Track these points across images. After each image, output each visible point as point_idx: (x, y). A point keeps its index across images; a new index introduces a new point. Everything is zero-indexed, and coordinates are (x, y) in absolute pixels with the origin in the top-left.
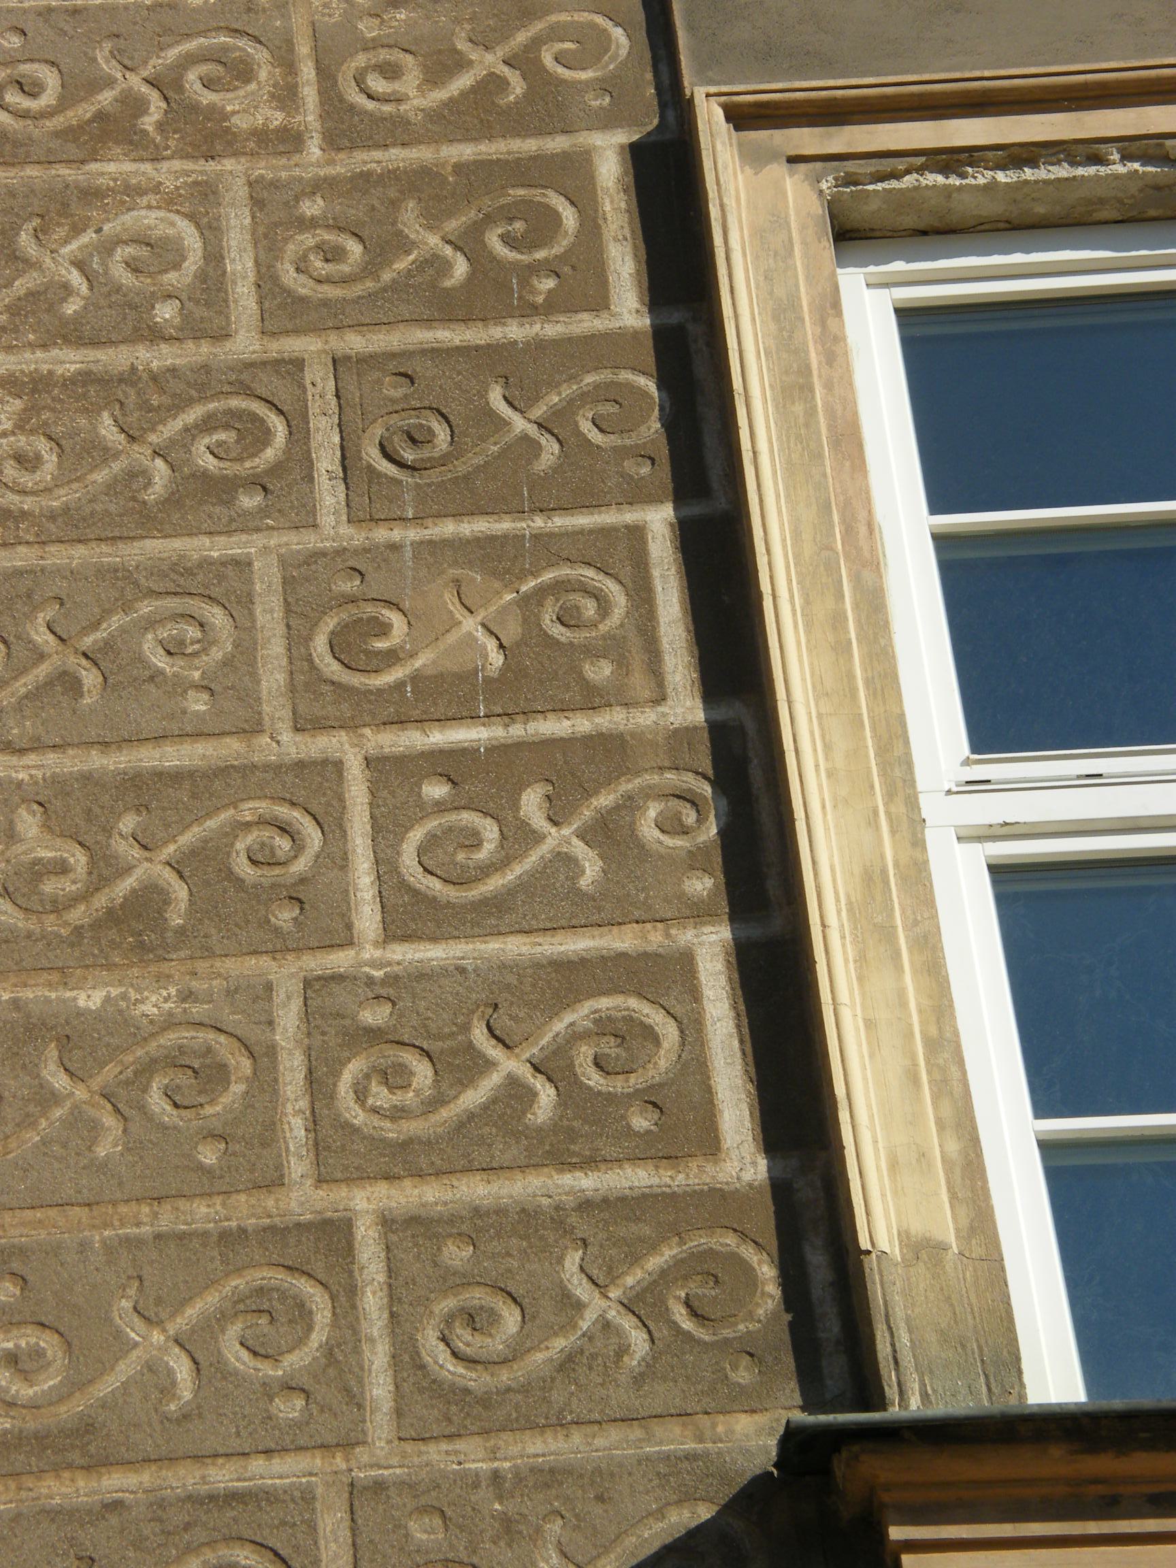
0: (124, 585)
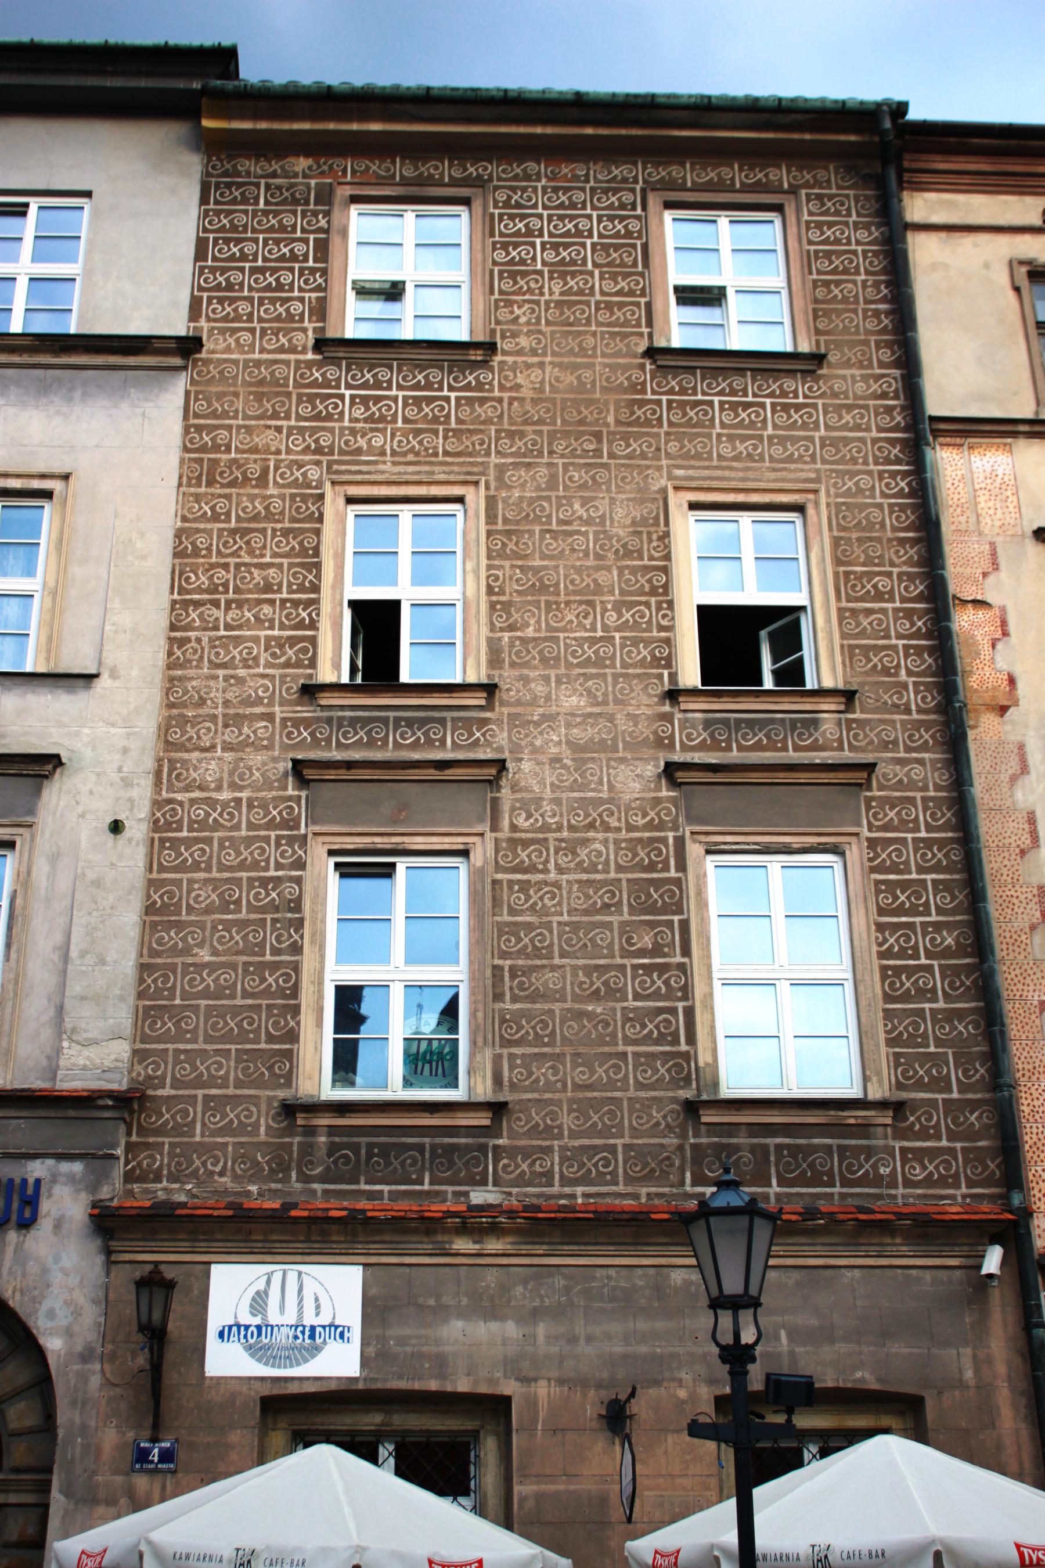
0: (594, 925)
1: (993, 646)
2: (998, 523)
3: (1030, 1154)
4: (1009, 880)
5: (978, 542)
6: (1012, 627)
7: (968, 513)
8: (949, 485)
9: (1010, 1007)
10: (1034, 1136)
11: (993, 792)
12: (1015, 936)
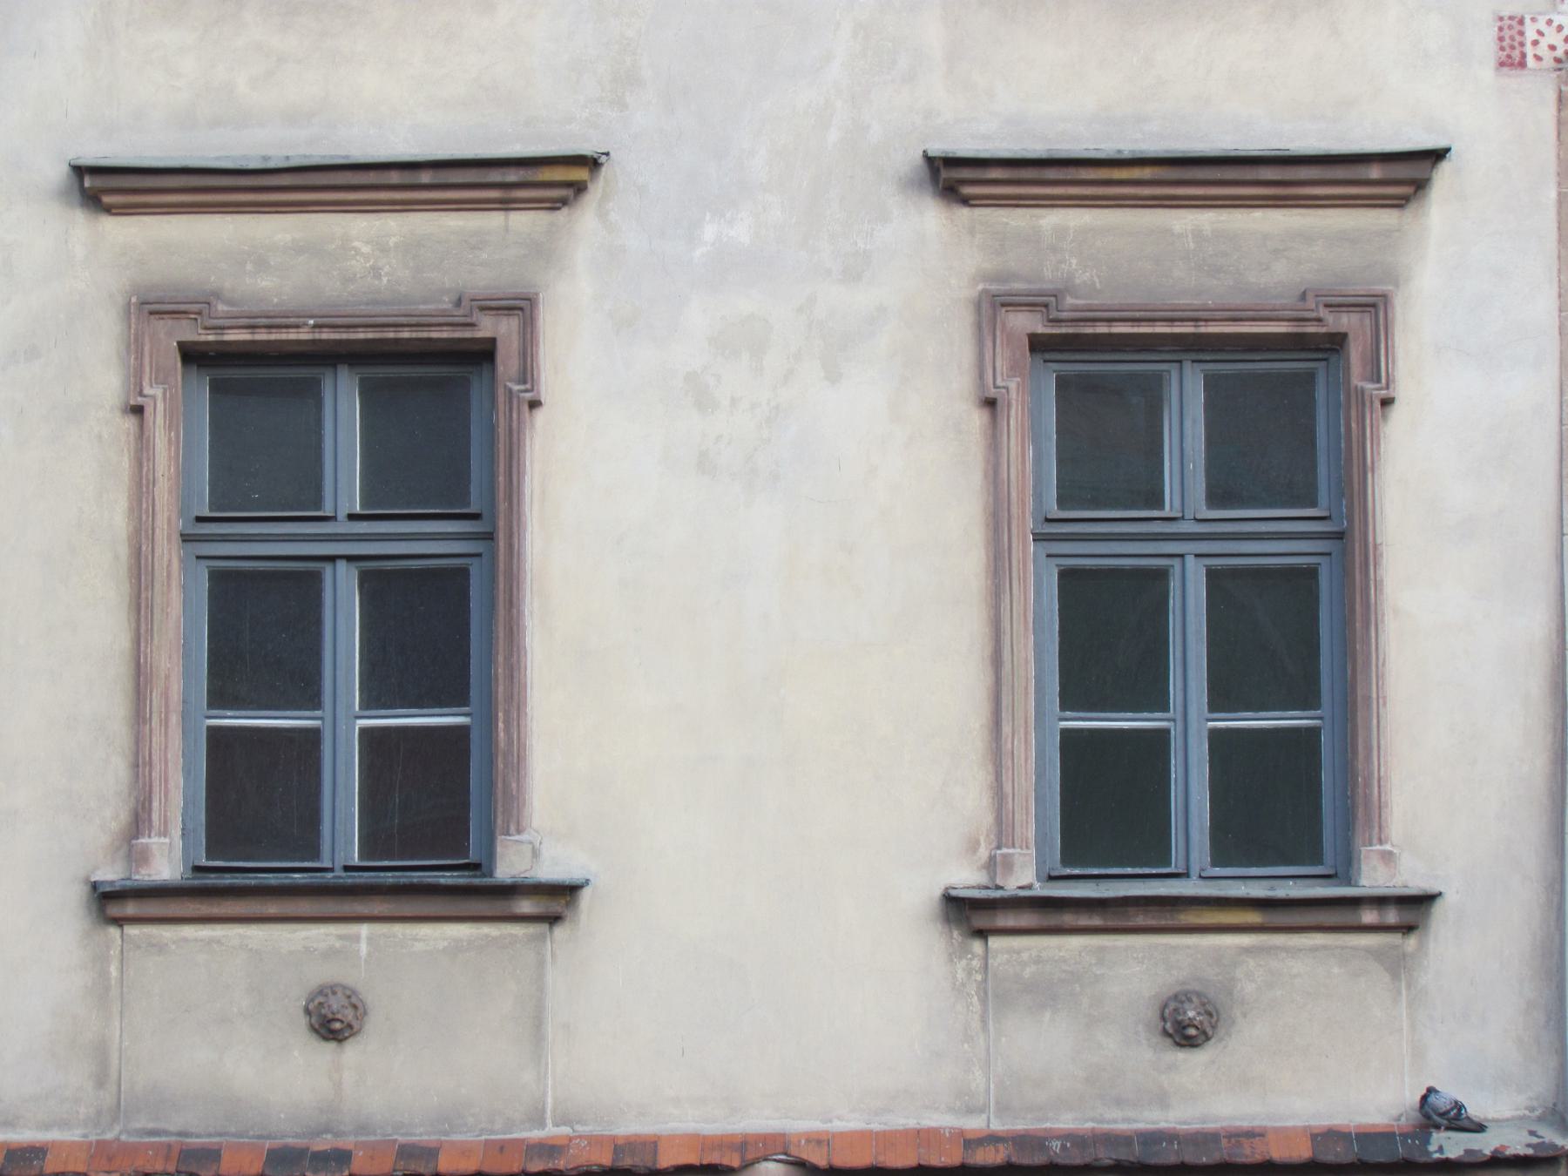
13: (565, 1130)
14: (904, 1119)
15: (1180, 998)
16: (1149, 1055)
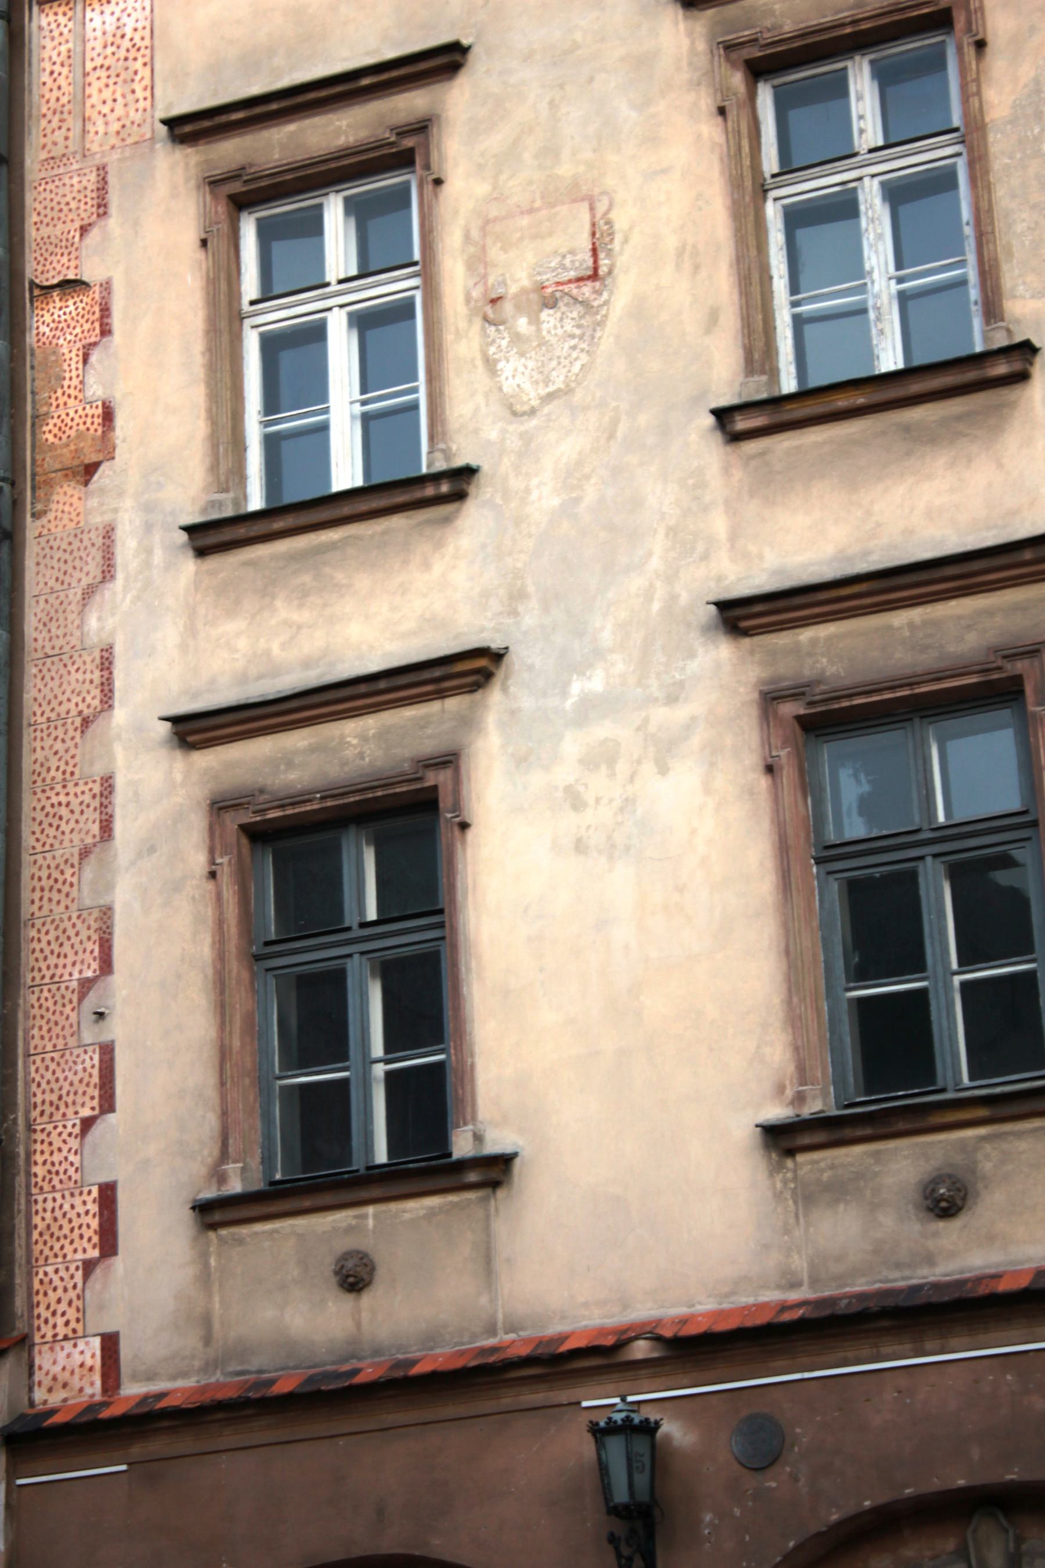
1: (85, 361)
2: (116, 126)
3: (40, 1246)
4: (59, 776)
5: (80, 173)
6: (117, 321)
7: (70, 122)
8: (45, 77)
9: (33, 999)
10: (48, 1215)
11: (53, 626)
12: (56, 874)
13: (512, 1336)
14: (746, 1299)
15: (936, 1181)
16: (917, 1227)
